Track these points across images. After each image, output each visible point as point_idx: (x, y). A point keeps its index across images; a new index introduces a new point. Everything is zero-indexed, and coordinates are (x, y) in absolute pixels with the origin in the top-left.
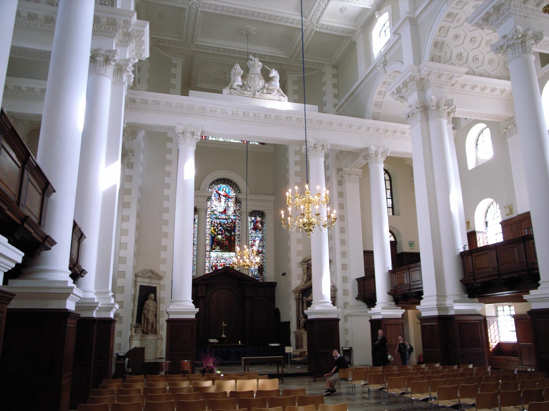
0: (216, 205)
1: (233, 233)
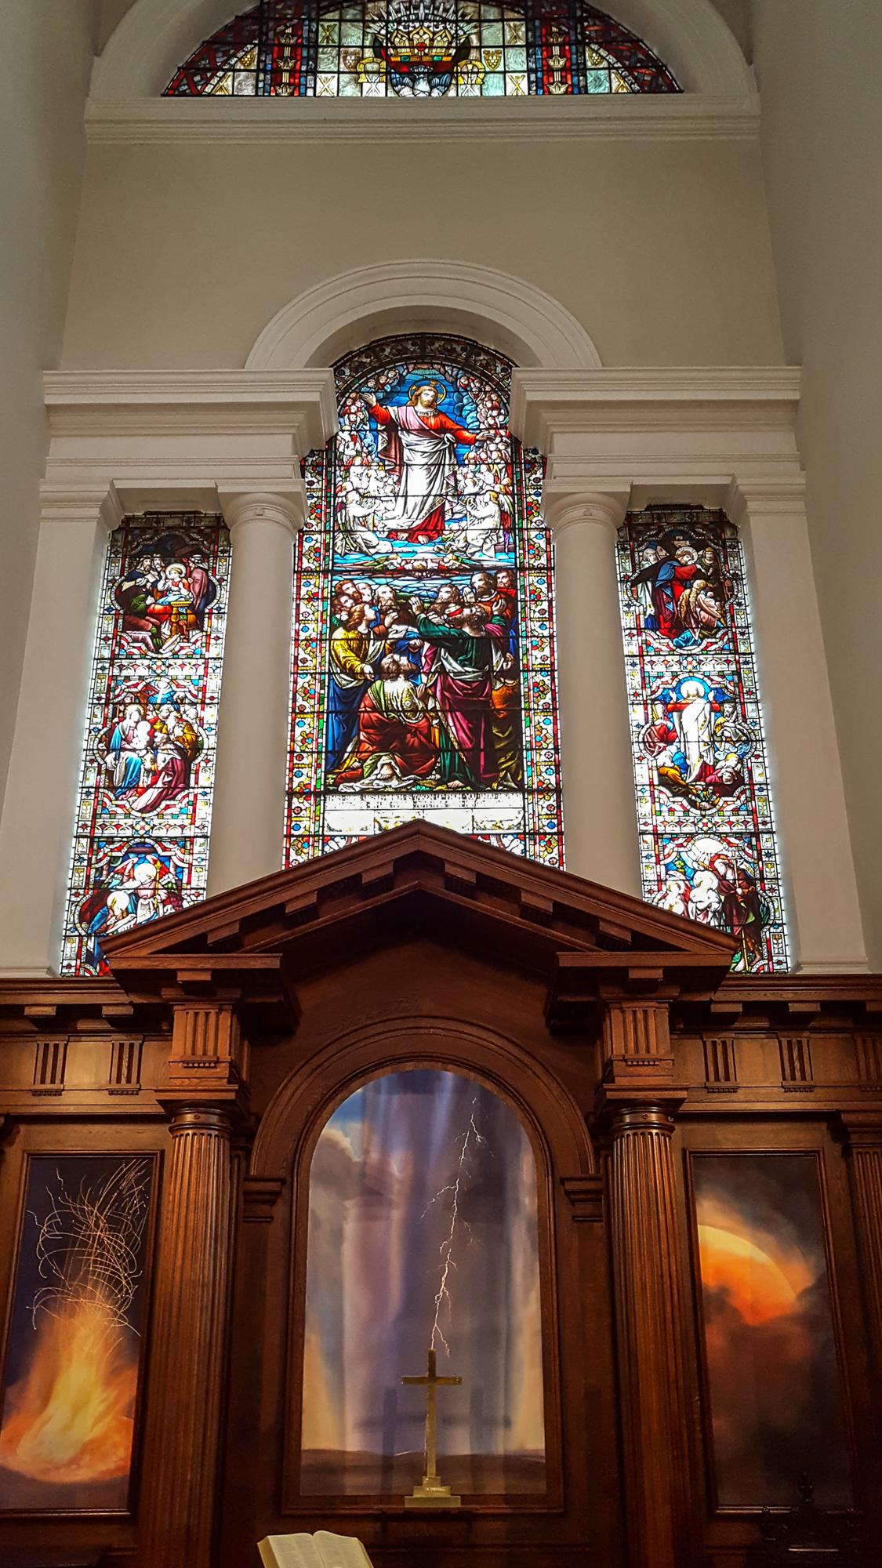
0: (373, 487)
1: (498, 661)
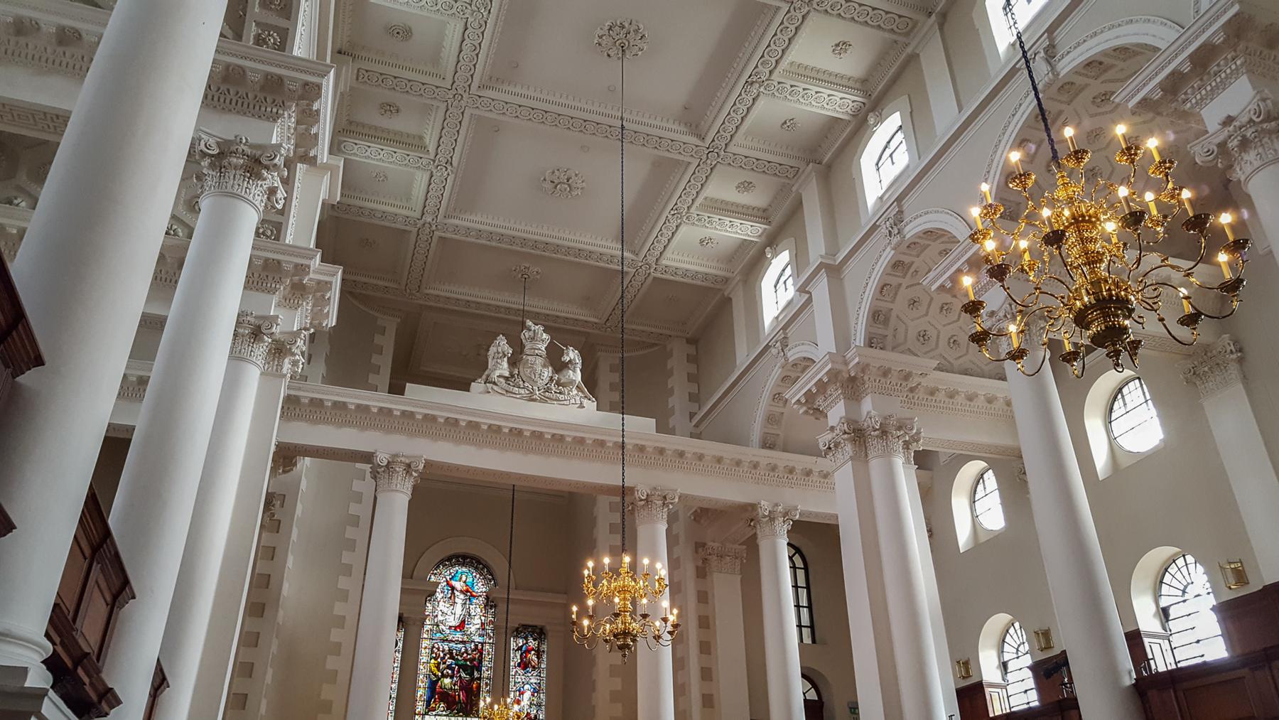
0: (445, 610)
